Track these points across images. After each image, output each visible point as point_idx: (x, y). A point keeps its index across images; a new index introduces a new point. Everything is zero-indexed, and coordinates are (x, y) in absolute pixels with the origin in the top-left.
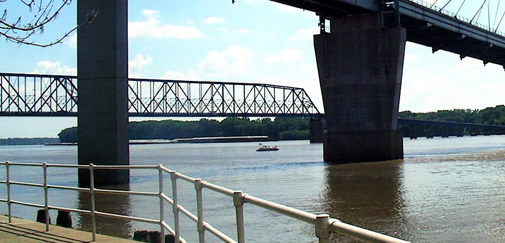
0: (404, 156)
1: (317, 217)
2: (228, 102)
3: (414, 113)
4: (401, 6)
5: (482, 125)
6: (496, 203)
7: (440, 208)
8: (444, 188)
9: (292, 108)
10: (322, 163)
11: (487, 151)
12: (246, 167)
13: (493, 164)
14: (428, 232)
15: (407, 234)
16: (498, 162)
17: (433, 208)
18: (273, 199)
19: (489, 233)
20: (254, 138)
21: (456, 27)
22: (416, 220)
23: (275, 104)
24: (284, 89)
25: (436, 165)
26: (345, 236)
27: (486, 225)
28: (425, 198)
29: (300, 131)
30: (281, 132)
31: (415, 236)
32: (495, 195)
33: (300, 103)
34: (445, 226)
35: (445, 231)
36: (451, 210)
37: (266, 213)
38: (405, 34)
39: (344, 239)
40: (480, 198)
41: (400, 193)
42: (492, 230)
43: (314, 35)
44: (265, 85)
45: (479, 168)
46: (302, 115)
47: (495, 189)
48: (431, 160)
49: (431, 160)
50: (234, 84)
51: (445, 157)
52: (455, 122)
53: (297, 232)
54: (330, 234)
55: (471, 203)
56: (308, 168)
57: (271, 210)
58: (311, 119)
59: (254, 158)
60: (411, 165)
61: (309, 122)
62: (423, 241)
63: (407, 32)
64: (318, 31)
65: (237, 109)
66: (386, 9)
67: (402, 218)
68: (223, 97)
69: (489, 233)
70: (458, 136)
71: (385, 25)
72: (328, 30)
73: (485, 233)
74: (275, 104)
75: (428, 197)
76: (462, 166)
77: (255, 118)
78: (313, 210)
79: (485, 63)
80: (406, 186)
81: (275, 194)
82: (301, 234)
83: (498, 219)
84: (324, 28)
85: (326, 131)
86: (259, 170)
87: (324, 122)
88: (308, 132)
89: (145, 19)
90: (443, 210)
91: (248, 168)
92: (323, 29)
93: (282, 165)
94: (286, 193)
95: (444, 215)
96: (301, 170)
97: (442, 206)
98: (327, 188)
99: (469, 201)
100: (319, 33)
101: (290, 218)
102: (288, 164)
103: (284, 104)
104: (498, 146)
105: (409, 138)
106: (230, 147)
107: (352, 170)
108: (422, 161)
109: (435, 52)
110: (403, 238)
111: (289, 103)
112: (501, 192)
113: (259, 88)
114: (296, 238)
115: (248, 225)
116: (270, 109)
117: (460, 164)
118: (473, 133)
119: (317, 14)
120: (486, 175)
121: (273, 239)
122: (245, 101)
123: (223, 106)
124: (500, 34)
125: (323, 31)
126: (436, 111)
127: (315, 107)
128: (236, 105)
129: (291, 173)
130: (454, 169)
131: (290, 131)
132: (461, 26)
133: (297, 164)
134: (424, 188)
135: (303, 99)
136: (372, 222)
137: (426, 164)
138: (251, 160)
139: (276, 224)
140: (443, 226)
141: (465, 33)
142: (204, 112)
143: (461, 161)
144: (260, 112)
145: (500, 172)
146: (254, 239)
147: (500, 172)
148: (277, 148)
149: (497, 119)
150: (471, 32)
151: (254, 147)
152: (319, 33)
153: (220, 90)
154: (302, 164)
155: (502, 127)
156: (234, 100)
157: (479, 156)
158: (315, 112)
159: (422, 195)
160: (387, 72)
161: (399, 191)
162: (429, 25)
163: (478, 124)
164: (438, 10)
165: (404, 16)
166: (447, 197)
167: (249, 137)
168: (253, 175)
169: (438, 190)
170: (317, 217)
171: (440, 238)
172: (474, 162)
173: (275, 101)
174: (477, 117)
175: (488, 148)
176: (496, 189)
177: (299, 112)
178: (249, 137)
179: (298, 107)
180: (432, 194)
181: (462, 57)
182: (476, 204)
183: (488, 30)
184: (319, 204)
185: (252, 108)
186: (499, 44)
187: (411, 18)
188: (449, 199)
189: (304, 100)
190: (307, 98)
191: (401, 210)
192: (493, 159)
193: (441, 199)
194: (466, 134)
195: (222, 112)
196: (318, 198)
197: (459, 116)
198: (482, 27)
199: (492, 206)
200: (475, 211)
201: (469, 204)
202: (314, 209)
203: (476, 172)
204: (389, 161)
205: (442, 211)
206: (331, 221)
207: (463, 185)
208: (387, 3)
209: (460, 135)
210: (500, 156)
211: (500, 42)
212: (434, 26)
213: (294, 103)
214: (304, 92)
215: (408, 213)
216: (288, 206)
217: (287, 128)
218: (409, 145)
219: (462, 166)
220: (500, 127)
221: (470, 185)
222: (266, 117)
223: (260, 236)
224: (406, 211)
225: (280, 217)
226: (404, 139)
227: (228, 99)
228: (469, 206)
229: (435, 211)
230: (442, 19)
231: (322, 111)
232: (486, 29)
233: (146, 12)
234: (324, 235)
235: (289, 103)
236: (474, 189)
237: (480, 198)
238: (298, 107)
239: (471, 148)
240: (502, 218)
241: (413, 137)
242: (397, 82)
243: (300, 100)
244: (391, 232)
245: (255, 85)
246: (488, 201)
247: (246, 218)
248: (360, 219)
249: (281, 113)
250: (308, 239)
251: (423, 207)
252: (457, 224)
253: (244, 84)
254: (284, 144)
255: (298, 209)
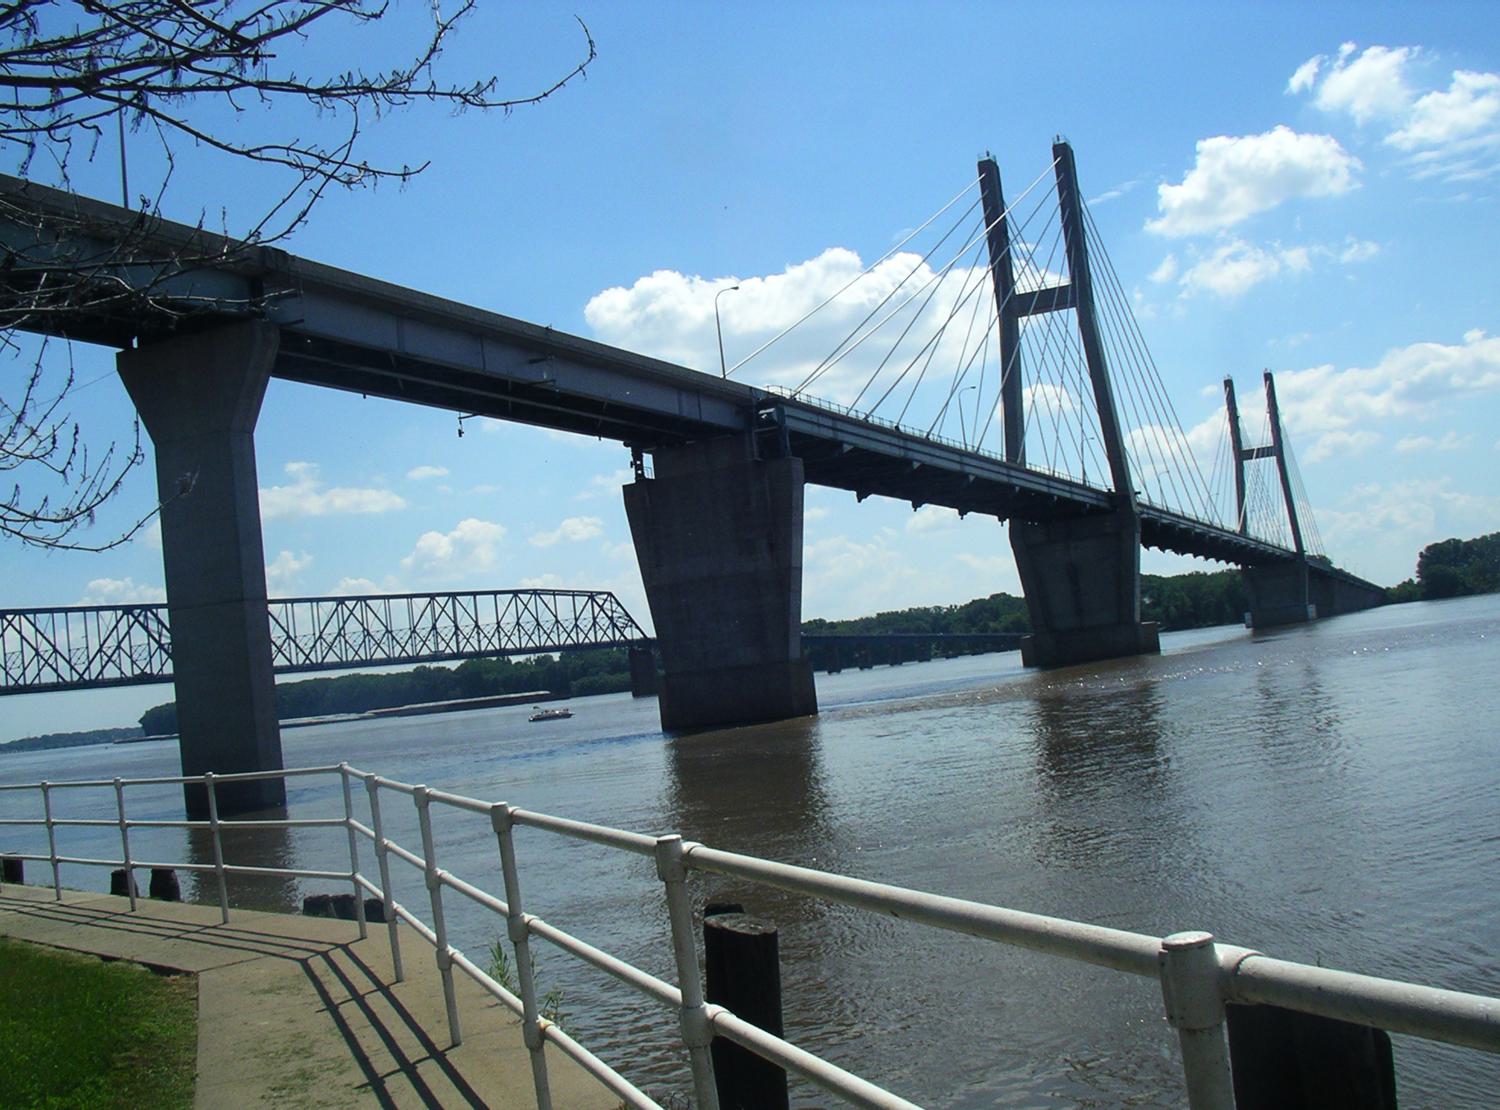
0: (819, 708)
1: (658, 842)
2: (467, 631)
3: (832, 623)
4: (789, 416)
5: (965, 635)
6: (1005, 786)
7: (896, 804)
8: (902, 765)
9: (592, 632)
10: (659, 734)
11: (981, 685)
12: (511, 754)
13: (994, 709)
14: (878, 853)
15: (837, 859)
16: (1004, 705)
17: (883, 806)
18: (569, 813)
19: (996, 846)
20: (523, 697)
21: (900, 447)
22: (851, 832)
23: (558, 628)
24: (573, 596)
25: (884, 720)
26: (714, 874)
27: (990, 831)
28: (866, 788)
29: (612, 674)
30: (575, 680)
31: (851, 862)
32: (1002, 770)
33: (606, 622)
34: (908, 838)
35: (912, 848)
36: (919, 805)
37: (558, 842)
38: (802, 468)
39: (715, 880)
40: (974, 779)
41: (817, 781)
42: (1003, 839)
43: (624, 487)
44: (535, 592)
45: (966, 719)
46: (613, 643)
47: (1002, 759)
48: (873, 711)
49: (873, 711)
50: (474, 594)
51: (898, 703)
52: (913, 634)
53: (621, 874)
54: (686, 873)
55: (956, 789)
56: (632, 747)
57: (568, 834)
58: (632, 653)
59: (525, 736)
60: (834, 725)
61: (627, 657)
62: (869, 871)
63: (804, 464)
64: (630, 478)
65: (484, 642)
66: (761, 423)
67: (825, 830)
68: (455, 622)
69: (996, 846)
70: (920, 661)
71: (761, 454)
72: (650, 474)
73: (989, 846)
74: (558, 628)
75: (872, 784)
76: (935, 718)
77: (521, 658)
78: (649, 829)
79: (962, 513)
80: (827, 767)
81: (572, 802)
82: (629, 878)
83: (1011, 816)
84: (642, 469)
85: (662, 672)
86: (537, 758)
87: (656, 653)
88: (626, 676)
89: (292, 480)
90: (904, 807)
91: (516, 757)
92: (640, 472)
93: (581, 746)
94: (593, 800)
95: (904, 818)
96: (618, 753)
97: (900, 801)
98: (674, 782)
99: (952, 786)
100: (634, 481)
101: (605, 847)
102: (593, 742)
103: (576, 626)
104: (999, 673)
105: (826, 673)
106: (385, 728)
107: (719, 744)
108: (856, 715)
109: (863, 500)
110: (829, 869)
111: (585, 622)
112: (1013, 764)
113: (525, 597)
114: (620, 885)
115: (524, 867)
116: (549, 637)
117: (929, 716)
118: (950, 652)
119: (626, 445)
120: (982, 732)
121: (575, 892)
122: (499, 626)
123: (457, 640)
124: (987, 454)
125: (640, 477)
126: (874, 615)
127: (638, 627)
128: (482, 635)
129: (601, 760)
130: (918, 726)
131: (592, 679)
132: (910, 445)
133: (610, 740)
134: (864, 768)
135: (613, 612)
136: (766, 843)
137: (863, 720)
138: (521, 741)
139: (579, 861)
140: (905, 838)
141: (919, 458)
142: (374, 657)
143: (931, 708)
144: (531, 644)
145: (1009, 724)
146: (539, 894)
147: (1009, 724)
148: (570, 712)
149: (994, 621)
150: (930, 455)
151: (523, 714)
152: (634, 481)
153: (449, 609)
154: (621, 739)
155: (1005, 637)
156: (477, 626)
157: (965, 696)
158: (638, 635)
159: (860, 783)
160: (772, 547)
161: (815, 778)
162: (847, 448)
163: (958, 634)
164: (862, 417)
165: (796, 435)
166: (908, 782)
167: (512, 695)
168: (525, 770)
169: (890, 770)
170: (658, 842)
171: (901, 864)
172: (957, 709)
173: (557, 621)
174: (956, 621)
175: (982, 679)
176: (1004, 759)
177: (606, 639)
178: (512, 695)
179: (604, 628)
180: (879, 779)
181: (916, 506)
182: (966, 792)
183: (963, 448)
184: (660, 815)
185: (515, 639)
186: (986, 474)
187: (811, 437)
188: (913, 786)
189: (615, 615)
190: (619, 609)
191: (821, 815)
192: (995, 701)
193: (897, 786)
194: (936, 656)
195: (455, 651)
196: (657, 804)
197: (921, 622)
198: (951, 443)
199: (998, 792)
200: (966, 805)
201: (952, 792)
202: (652, 827)
203: (962, 728)
204: (790, 720)
205: (902, 810)
206: (686, 846)
207: (939, 755)
208: (761, 412)
209: (924, 657)
210: (1006, 693)
211: (988, 470)
212: (856, 450)
213: (595, 623)
214: (613, 600)
215: (836, 819)
216: (599, 824)
217: (584, 671)
218: (826, 686)
219: (935, 718)
220: (1001, 637)
221: (952, 755)
222: (543, 655)
223: (549, 887)
224: (830, 815)
225: (587, 847)
226: (816, 674)
227: (466, 624)
228: (953, 795)
229: (889, 811)
230: (872, 434)
231: (651, 633)
232: (957, 445)
233: (293, 467)
234: (675, 876)
235: (585, 622)
236: (960, 761)
237: (974, 779)
238: (604, 628)
239: (947, 682)
240: (1020, 814)
241: (834, 668)
242: (794, 565)
243: (607, 616)
244: (805, 858)
245: (516, 593)
246: (990, 783)
247: (520, 854)
248: (743, 839)
249: (608, 639)
250: (644, 886)
251: (863, 804)
252: (934, 833)
253: (495, 593)
254: (581, 704)
255: (619, 828)
